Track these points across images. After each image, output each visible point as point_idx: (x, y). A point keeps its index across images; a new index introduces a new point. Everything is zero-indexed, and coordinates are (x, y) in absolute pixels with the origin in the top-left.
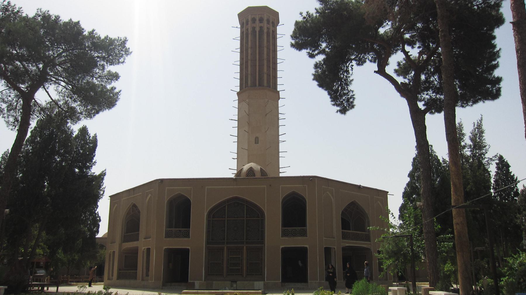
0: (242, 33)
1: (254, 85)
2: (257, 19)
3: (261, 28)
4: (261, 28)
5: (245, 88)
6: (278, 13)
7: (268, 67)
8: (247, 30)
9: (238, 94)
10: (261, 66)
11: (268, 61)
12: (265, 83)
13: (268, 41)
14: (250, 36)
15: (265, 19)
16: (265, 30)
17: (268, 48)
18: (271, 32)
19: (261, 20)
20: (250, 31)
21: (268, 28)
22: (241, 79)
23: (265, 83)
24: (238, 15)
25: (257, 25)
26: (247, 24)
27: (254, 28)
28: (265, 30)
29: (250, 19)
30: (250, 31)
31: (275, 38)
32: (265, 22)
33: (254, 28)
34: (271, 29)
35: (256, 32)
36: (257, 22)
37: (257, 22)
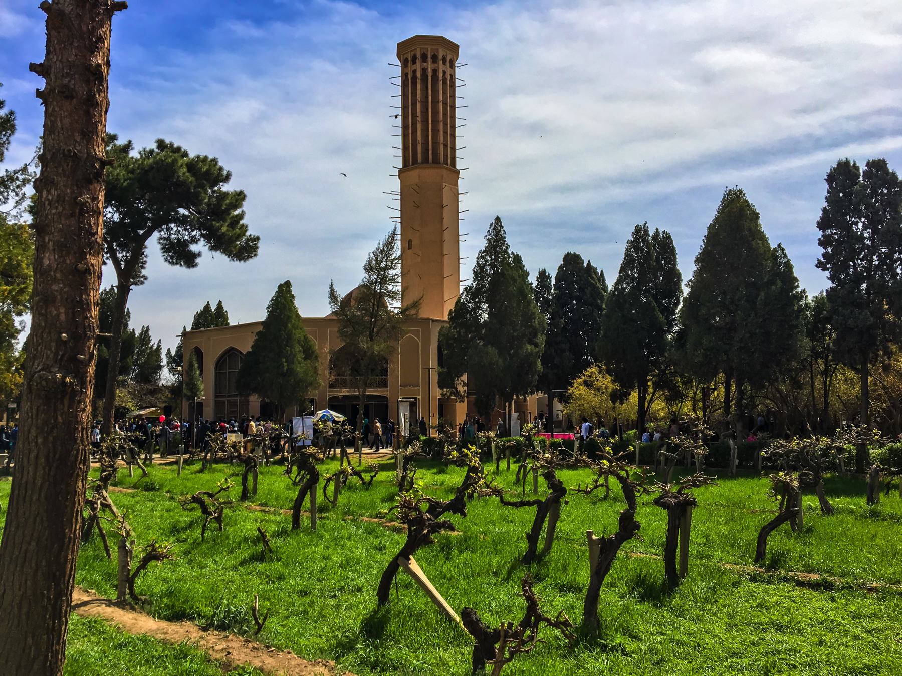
0: (405, 76)
1: (426, 160)
2: (429, 56)
3: (435, 71)
4: (435, 71)
5: (413, 164)
6: (458, 46)
7: (445, 132)
8: (414, 71)
9: (401, 171)
10: (436, 131)
11: (445, 124)
12: (442, 160)
13: (445, 93)
14: (419, 81)
15: (440, 57)
16: (441, 75)
17: (445, 104)
18: (449, 78)
19: (435, 58)
20: (419, 75)
21: (444, 72)
22: (405, 148)
23: (442, 160)
24: (398, 44)
25: (430, 66)
26: (414, 62)
27: (424, 70)
28: (441, 75)
29: (419, 56)
30: (419, 75)
31: (453, 86)
32: (441, 62)
33: (424, 70)
34: (449, 72)
35: (427, 76)
36: (430, 60)
37: (430, 60)
